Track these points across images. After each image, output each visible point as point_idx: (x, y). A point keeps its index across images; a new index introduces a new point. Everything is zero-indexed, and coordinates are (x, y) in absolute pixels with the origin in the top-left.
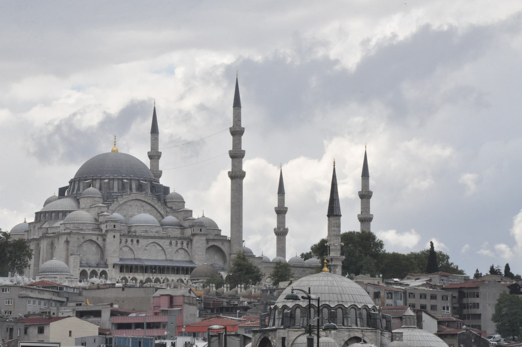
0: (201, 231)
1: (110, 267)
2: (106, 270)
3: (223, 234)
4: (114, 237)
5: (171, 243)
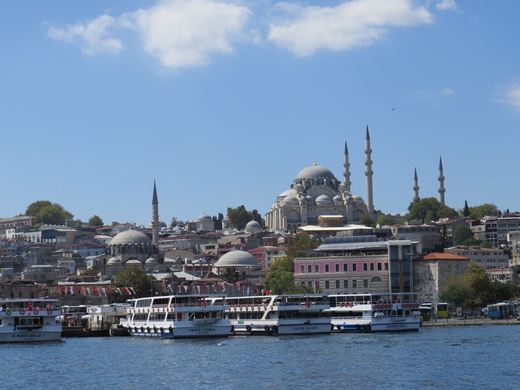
4: (304, 207)
5: (335, 209)
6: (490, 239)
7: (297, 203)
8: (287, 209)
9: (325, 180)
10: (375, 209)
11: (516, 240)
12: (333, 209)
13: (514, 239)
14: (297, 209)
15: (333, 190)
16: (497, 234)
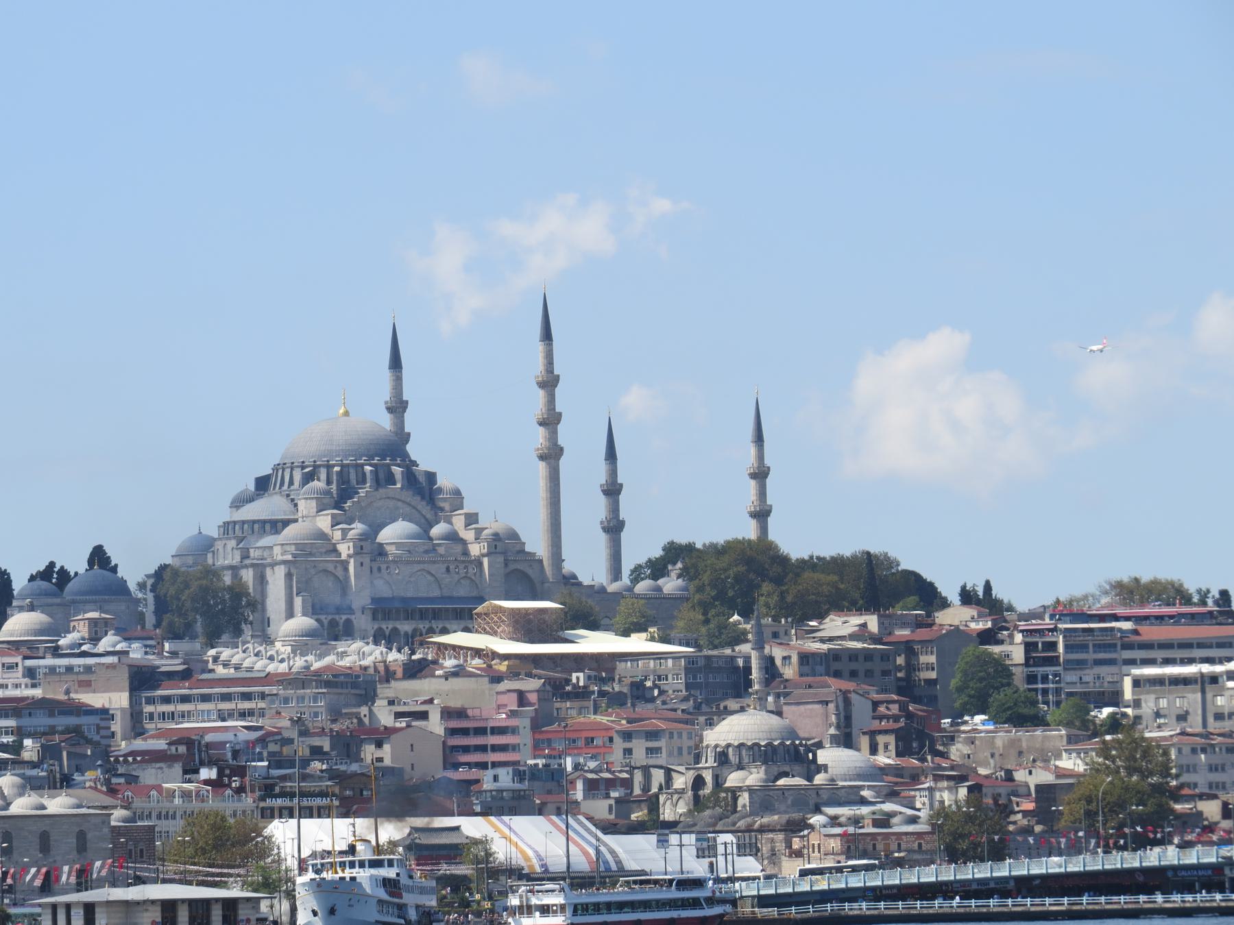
0: (496, 548)
2: (352, 617)
3: (528, 549)
4: (362, 564)
5: (448, 569)
6: (1040, 686)
7: (331, 548)
8: (306, 569)
9: (368, 468)
10: (568, 567)
11: (1153, 697)
12: (443, 567)
13: (1148, 693)
14: (336, 567)
15: (424, 503)
16: (1062, 672)
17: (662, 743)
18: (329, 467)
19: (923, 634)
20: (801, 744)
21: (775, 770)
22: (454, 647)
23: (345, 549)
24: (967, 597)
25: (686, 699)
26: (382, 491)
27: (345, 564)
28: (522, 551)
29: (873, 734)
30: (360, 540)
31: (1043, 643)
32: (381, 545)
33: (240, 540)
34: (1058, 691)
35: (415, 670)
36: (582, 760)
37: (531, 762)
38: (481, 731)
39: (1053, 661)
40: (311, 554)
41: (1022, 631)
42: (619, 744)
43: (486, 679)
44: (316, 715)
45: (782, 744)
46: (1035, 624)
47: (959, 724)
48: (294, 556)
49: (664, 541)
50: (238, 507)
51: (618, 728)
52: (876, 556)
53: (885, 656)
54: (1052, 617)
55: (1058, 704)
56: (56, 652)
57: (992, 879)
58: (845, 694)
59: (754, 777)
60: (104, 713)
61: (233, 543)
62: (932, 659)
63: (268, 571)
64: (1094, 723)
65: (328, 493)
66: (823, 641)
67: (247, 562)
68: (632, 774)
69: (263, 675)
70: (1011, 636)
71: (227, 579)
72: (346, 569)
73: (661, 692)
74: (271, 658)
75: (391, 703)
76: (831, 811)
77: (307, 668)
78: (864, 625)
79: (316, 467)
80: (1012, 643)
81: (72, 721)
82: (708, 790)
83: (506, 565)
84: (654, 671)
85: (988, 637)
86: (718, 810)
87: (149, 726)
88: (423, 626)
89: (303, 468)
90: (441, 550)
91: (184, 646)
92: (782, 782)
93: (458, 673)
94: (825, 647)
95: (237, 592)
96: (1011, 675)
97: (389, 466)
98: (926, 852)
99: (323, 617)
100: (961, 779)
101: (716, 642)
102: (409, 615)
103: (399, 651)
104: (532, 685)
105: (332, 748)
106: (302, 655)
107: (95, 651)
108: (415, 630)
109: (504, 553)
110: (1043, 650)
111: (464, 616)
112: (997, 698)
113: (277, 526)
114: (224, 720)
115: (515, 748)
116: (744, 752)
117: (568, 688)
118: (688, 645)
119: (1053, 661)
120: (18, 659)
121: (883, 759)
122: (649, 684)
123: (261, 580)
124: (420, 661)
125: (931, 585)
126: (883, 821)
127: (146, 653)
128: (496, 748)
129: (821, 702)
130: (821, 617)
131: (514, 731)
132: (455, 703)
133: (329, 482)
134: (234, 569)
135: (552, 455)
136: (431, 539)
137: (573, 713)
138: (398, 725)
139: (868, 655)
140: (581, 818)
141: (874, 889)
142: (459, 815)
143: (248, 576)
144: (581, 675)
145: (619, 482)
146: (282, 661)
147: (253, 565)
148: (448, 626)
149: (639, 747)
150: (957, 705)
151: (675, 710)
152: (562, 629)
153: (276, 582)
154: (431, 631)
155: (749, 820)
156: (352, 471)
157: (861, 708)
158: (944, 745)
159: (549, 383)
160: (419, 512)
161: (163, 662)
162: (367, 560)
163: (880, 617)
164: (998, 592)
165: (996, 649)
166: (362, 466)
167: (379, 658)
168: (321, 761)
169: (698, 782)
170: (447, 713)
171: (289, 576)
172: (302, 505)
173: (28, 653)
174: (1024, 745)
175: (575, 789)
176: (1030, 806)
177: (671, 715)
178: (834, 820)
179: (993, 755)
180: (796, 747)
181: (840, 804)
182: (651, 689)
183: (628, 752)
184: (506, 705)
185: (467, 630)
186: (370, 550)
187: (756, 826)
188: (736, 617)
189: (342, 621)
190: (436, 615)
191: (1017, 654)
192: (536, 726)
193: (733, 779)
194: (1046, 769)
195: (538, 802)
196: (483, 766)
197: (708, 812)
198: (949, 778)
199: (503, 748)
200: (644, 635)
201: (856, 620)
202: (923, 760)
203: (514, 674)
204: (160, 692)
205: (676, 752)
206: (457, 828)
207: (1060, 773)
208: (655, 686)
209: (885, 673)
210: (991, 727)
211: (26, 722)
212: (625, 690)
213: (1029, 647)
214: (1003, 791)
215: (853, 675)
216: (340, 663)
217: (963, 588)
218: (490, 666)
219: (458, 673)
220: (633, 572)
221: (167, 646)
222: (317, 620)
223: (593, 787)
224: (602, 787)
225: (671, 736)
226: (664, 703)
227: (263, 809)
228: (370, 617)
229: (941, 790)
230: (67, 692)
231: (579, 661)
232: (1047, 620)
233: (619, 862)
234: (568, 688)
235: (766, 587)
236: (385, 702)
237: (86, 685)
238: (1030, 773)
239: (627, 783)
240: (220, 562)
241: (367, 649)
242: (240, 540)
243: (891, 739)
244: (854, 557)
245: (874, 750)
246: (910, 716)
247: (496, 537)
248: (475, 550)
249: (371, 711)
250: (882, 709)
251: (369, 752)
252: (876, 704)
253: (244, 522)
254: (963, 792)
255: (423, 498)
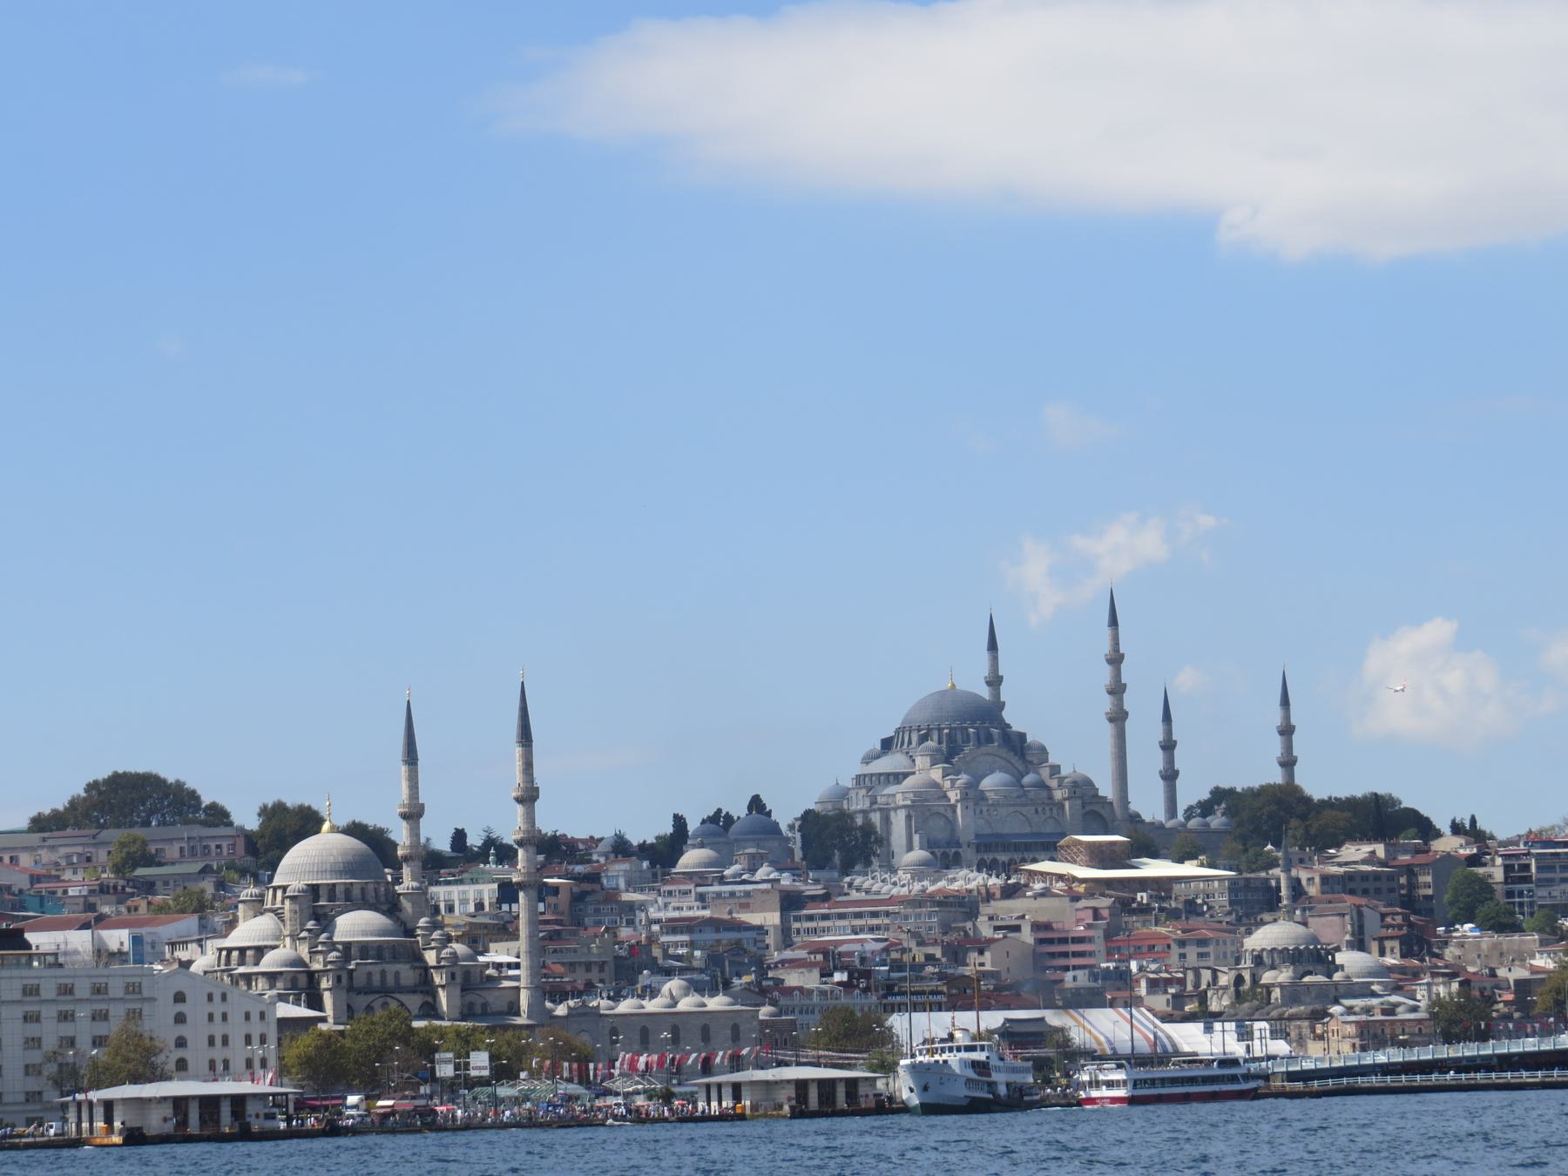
1: (965, 847)
2: (960, 850)
3: (1101, 793)
5: (1037, 812)
6: (1517, 900)
10: (1133, 807)
12: (1032, 809)
15: (1017, 758)
17: (1210, 949)
18: (940, 730)
19: (1421, 859)
20: (1322, 948)
21: (1301, 969)
22: (1042, 873)
23: (953, 796)
24: (1457, 829)
25: (1229, 913)
26: (983, 749)
27: (953, 808)
28: (1096, 795)
29: (1381, 940)
30: (966, 788)
31: (1519, 865)
32: (982, 792)
33: (869, 789)
34: (1531, 904)
35: (1010, 892)
36: (1145, 963)
37: (1104, 965)
38: (1064, 941)
39: (1527, 880)
40: (926, 800)
41: (1501, 856)
42: (1175, 950)
43: (1067, 899)
44: (930, 929)
45: (1307, 948)
46: (1512, 849)
47: (1451, 932)
48: (913, 801)
49: (1210, 787)
50: (867, 763)
51: (1174, 937)
52: (1382, 797)
53: (1391, 877)
54: (1526, 844)
55: (1532, 914)
56: (722, 880)
57: (1479, 1056)
58: (1358, 907)
59: (1284, 975)
60: (760, 929)
61: (863, 792)
62: (1429, 879)
63: (892, 814)
64: (1561, 929)
65: (938, 750)
66: (1340, 865)
67: (876, 806)
68: (1185, 974)
69: (888, 897)
70: (1493, 860)
71: (859, 821)
72: (954, 811)
73: (1210, 908)
74: (895, 884)
75: (991, 918)
76: (1348, 1002)
77: (924, 891)
78: (1373, 852)
79: (929, 730)
80: (1493, 865)
81: (734, 935)
82: (1247, 985)
83: (1083, 807)
84: (1204, 891)
85: (1474, 861)
86: (1256, 1003)
87: (797, 939)
88: (1017, 856)
89: (919, 731)
90: (1031, 795)
91: (823, 874)
92: (1307, 979)
93: (1045, 893)
94: (1342, 870)
95: (868, 829)
96: (1492, 891)
97: (987, 728)
98: (1425, 1035)
99: (936, 850)
100: (1453, 976)
101: (1254, 867)
102: (1006, 847)
103: (998, 877)
104: (1104, 903)
105: (943, 955)
106: (919, 881)
107: (753, 879)
108: (1011, 860)
109: (1081, 797)
110: (1519, 872)
111: (1050, 847)
112: (1482, 910)
113: (898, 777)
114: (856, 933)
115: (1091, 954)
116: (1275, 955)
117: (1134, 905)
118: (1231, 870)
119: (1527, 880)
120: (691, 887)
121: (1390, 960)
122: (1199, 901)
123: (887, 821)
124: (1014, 885)
125: (1427, 819)
126: (1390, 1010)
127: (794, 881)
128: (1076, 954)
129: (1339, 914)
130: (1338, 846)
131: (1090, 940)
132: (1043, 918)
133: (940, 742)
134: (864, 812)
135: (1118, 718)
136: (1022, 786)
137: (1138, 925)
138: (996, 936)
139: (1376, 876)
140: (1143, 1009)
141: (1381, 1066)
142: (1045, 1008)
143: (876, 818)
144: (1144, 895)
145: (1002, 700)
146: (903, 886)
147: (880, 809)
148: (1038, 857)
149: (1192, 952)
150: (1450, 916)
151: (1221, 922)
152: (1129, 858)
153: (899, 821)
154: (1024, 861)
155: (1280, 1010)
156: (958, 732)
157: (1371, 918)
158: (1439, 948)
159: (1116, 659)
160: (1012, 764)
161: (808, 887)
162: (971, 804)
163: (1386, 846)
164: (1481, 825)
165: (1481, 870)
166: (966, 728)
167: (982, 882)
168: (934, 966)
169: (1239, 980)
170: (1037, 927)
171: (909, 817)
172: (918, 760)
173: (700, 881)
174: (1505, 947)
175: (1140, 987)
176: (1510, 997)
177: (1218, 926)
178: (1350, 1010)
179: (1479, 956)
180: (1318, 950)
181: (1355, 997)
182: (1202, 905)
183: (1183, 956)
184: (1083, 920)
185: (1053, 859)
186: (972, 795)
187: (1286, 1015)
188: (1269, 847)
189: (951, 854)
190: (1027, 847)
191: (1498, 874)
192: (1109, 935)
193: (1267, 977)
194: (1523, 966)
195: (1109, 997)
196: (1066, 969)
197: (1246, 1005)
198: (1444, 975)
199: (1081, 954)
200: (1195, 862)
201: (1366, 849)
202: (1422, 960)
203: (1090, 894)
204: (805, 912)
205: (1221, 956)
206: (1042, 1020)
207: (1534, 970)
208: (1205, 903)
209: (1391, 890)
210: (1478, 934)
211: (697, 936)
212: (1180, 906)
213: (1508, 868)
214: (1488, 985)
215: (1365, 892)
216: (951, 887)
217: (1453, 822)
218: (1070, 888)
219: (1045, 893)
220: (1186, 811)
221: (811, 874)
222: (931, 853)
223: (1154, 985)
224: (1161, 985)
225: (1218, 943)
226: (1212, 916)
227: (885, 1005)
228: (974, 850)
229: (1437, 984)
230: (730, 913)
231: (1143, 883)
232: (1522, 847)
233: (1174, 1045)
234: (1134, 905)
235: (1294, 822)
236: (986, 918)
237: (745, 907)
238: (1510, 970)
239: (1182, 982)
240: (853, 808)
241: (971, 875)
242: (869, 789)
243: (1396, 944)
244: (1365, 797)
245: (1382, 953)
246: (1411, 925)
247: (1075, 785)
248: (1058, 795)
249: (974, 925)
250: (1389, 920)
251: (973, 957)
252: (1383, 916)
253: (872, 775)
254: (1455, 986)
255: (1016, 754)
